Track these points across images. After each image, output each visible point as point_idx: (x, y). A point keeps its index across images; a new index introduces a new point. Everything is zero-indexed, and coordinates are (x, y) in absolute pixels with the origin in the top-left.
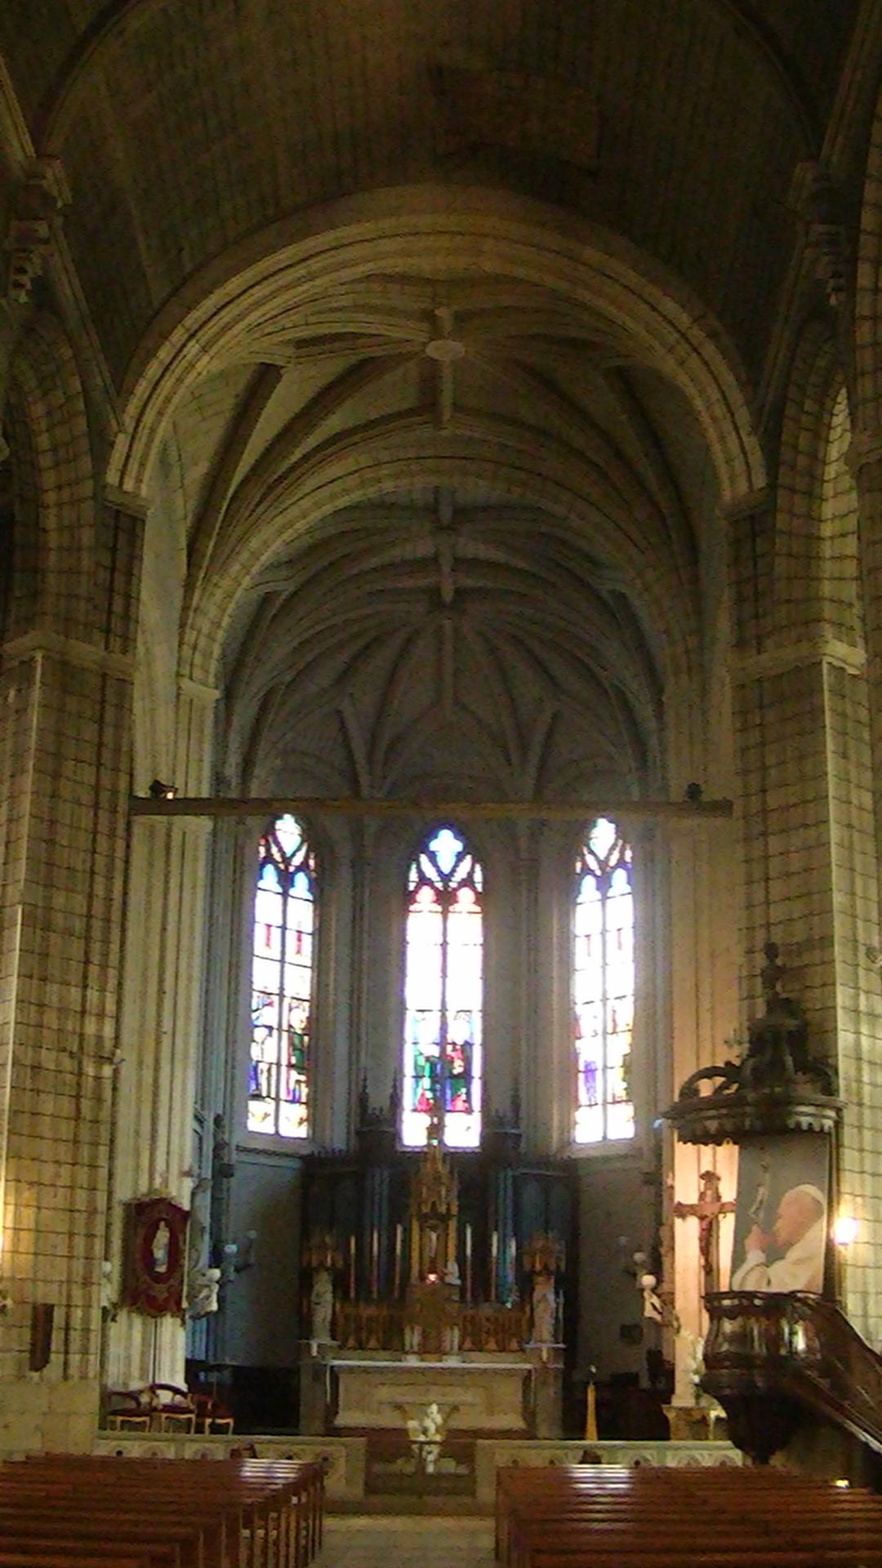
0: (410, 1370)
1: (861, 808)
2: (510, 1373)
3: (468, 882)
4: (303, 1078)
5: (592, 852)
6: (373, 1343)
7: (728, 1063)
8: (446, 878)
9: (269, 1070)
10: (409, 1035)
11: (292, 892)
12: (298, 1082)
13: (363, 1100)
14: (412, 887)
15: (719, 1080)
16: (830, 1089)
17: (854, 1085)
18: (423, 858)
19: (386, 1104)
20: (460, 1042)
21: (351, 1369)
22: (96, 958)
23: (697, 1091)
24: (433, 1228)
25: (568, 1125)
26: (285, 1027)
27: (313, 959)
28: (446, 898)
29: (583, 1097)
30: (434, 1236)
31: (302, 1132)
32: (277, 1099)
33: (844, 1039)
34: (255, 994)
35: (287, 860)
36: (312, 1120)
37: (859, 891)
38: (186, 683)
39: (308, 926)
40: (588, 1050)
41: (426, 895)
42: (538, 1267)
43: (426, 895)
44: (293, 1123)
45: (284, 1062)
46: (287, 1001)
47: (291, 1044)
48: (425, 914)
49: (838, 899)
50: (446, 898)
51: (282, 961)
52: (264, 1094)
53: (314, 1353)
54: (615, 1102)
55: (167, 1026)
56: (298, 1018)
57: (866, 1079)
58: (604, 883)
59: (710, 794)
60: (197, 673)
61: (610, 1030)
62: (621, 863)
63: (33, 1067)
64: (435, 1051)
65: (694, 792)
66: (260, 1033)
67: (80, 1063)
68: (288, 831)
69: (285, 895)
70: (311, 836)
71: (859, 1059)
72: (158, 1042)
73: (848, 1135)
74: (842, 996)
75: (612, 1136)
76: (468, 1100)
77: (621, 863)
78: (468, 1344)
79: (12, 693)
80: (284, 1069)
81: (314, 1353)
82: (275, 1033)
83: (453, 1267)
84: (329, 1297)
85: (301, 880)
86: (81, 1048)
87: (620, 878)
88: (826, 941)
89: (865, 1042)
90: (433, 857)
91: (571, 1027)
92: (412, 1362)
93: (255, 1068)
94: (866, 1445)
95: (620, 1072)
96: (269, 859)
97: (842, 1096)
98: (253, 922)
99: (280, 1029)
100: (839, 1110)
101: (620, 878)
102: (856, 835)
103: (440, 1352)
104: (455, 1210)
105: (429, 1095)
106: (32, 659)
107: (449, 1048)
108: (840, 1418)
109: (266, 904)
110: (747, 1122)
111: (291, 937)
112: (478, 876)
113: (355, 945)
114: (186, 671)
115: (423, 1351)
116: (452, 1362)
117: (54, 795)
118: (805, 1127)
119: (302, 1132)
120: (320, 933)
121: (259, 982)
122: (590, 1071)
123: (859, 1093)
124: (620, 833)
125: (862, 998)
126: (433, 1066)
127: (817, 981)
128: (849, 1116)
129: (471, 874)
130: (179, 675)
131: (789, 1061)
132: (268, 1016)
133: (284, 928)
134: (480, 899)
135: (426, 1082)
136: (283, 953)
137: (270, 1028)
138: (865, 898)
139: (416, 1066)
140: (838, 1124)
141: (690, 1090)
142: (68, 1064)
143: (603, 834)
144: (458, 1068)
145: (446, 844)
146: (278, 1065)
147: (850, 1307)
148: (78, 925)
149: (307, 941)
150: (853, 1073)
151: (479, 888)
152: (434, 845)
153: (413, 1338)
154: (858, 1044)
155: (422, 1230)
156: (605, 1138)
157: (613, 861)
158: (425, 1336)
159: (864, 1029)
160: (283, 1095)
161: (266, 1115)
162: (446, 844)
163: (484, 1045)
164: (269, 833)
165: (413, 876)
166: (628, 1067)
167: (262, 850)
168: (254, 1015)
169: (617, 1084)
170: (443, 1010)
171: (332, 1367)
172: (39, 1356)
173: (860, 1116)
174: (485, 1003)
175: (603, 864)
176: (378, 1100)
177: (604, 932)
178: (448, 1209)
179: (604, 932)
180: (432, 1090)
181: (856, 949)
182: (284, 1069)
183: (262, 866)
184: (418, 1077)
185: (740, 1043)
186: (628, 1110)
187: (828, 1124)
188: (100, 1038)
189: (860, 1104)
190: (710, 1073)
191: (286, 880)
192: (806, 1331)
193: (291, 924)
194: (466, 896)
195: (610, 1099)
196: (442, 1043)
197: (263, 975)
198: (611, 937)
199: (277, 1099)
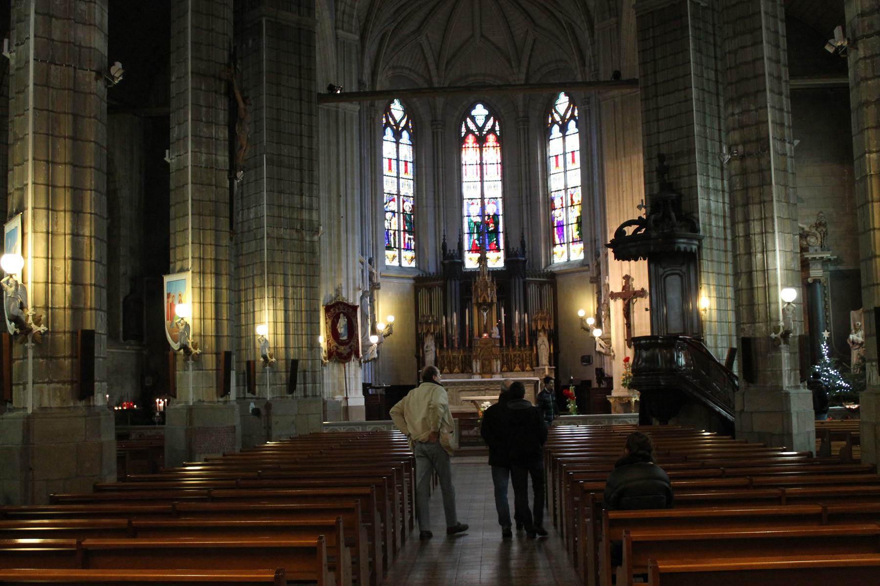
1: (708, 80)
3: (492, 131)
4: (412, 237)
5: (556, 112)
6: (456, 370)
7: (640, 218)
8: (481, 129)
9: (394, 234)
10: (465, 213)
11: (401, 141)
12: (409, 239)
13: (444, 247)
14: (463, 134)
15: (635, 227)
16: (694, 229)
17: (707, 227)
18: (468, 120)
19: (456, 248)
20: (492, 214)
22: (306, 180)
23: (625, 232)
24: (485, 310)
25: (550, 255)
28: (481, 141)
29: (557, 241)
31: (413, 264)
32: (399, 249)
33: (702, 203)
35: (397, 124)
36: (417, 258)
37: (708, 125)
38: (340, 32)
39: (410, 158)
40: (558, 215)
41: (471, 139)
43: (471, 139)
47: (404, 219)
49: (696, 128)
50: (481, 141)
51: (398, 177)
54: (573, 242)
55: (343, 213)
56: (408, 206)
57: (713, 224)
58: (564, 129)
59: (625, 76)
60: (346, 26)
61: (570, 204)
62: (572, 117)
63: (278, 239)
64: (479, 219)
65: (617, 75)
66: (389, 215)
67: (302, 235)
68: (397, 110)
69: (397, 143)
70: (407, 111)
71: (710, 213)
72: (339, 222)
73: (705, 253)
74: (700, 181)
75: (572, 259)
76: (498, 243)
77: (572, 117)
78: (505, 369)
79: (250, 42)
83: (496, 330)
84: (433, 348)
85: (405, 134)
86: (302, 227)
87: (572, 125)
88: (691, 152)
89: (713, 205)
90: (473, 119)
91: (550, 204)
92: (477, 378)
93: (387, 233)
94: (719, 413)
95: (575, 227)
96: (388, 124)
97: (701, 233)
98: (382, 157)
99: (398, 212)
100: (700, 240)
101: (572, 125)
102: (706, 95)
103: (491, 373)
104: (495, 300)
105: (477, 242)
106: (260, 24)
107: (486, 218)
108: (705, 400)
109: (388, 148)
110: (652, 248)
111: (402, 164)
112: (497, 128)
113: (435, 168)
114: (340, 24)
115: (483, 373)
117: (278, 95)
118: (682, 249)
119: (413, 264)
120: (416, 162)
121: (387, 189)
122: (560, 226)
123: (711, 232)
124: (571, 101)
125: (711, 181)
126: (478, 227)
127: (685, 173)
128: (705, 243)
129: (494, 126)
130: (336, 28)
131: (673, 214)
132: (393, 206)
133: (398, 160)
134: (499, 140)
135: (476, 236)
136: (398, 173)
137: (393, 212)
138: (712, 128)
140: (700, 247)
141: (620, 232)
142: (295, 235)
143: (562, 102)
144: (491, 227)
145: (480, 112)
146: (399, 231)
147: (708, 342)
148: (296, 163)
149: (410, 166)
150: (707, 220)
151: (498, 133)
152: (473, 113)
153: (477, 366)
154: (709, 205)
155: (479, 311)
156: (569, 260)
157: (568, 116)
158: (483, 366)
159: (712, 198)
160: (402, 247)
161: (394, 257)
162: (480, 112)
163: (504, 215)
164: (388, 110)
165: (464, 129)
166: (579, 222)
167: (384, 120)
169: (573, 232)
170: (482, 198)
172: (291, 386)
173: (711, 242)
174: (504, 192)
175: (563, 118)
176: (452, 246)
177: (565, 154)
179: (565, 154)
180: (478, 239)
181: (707, 156)
183: (385, 128)
184: (470, 234)
185: (645, 207)
186: (581, 246)
187: (694, 247)
188: (311, 221)
189: (711, 237)
190: (629, 223)
191: (397, 135)
192: (685, 356)
193: (402, 158)
194: (491, 138)
196: (482, 214)
197: (389, 186)
198: (569, 157)
199: (399, 249)
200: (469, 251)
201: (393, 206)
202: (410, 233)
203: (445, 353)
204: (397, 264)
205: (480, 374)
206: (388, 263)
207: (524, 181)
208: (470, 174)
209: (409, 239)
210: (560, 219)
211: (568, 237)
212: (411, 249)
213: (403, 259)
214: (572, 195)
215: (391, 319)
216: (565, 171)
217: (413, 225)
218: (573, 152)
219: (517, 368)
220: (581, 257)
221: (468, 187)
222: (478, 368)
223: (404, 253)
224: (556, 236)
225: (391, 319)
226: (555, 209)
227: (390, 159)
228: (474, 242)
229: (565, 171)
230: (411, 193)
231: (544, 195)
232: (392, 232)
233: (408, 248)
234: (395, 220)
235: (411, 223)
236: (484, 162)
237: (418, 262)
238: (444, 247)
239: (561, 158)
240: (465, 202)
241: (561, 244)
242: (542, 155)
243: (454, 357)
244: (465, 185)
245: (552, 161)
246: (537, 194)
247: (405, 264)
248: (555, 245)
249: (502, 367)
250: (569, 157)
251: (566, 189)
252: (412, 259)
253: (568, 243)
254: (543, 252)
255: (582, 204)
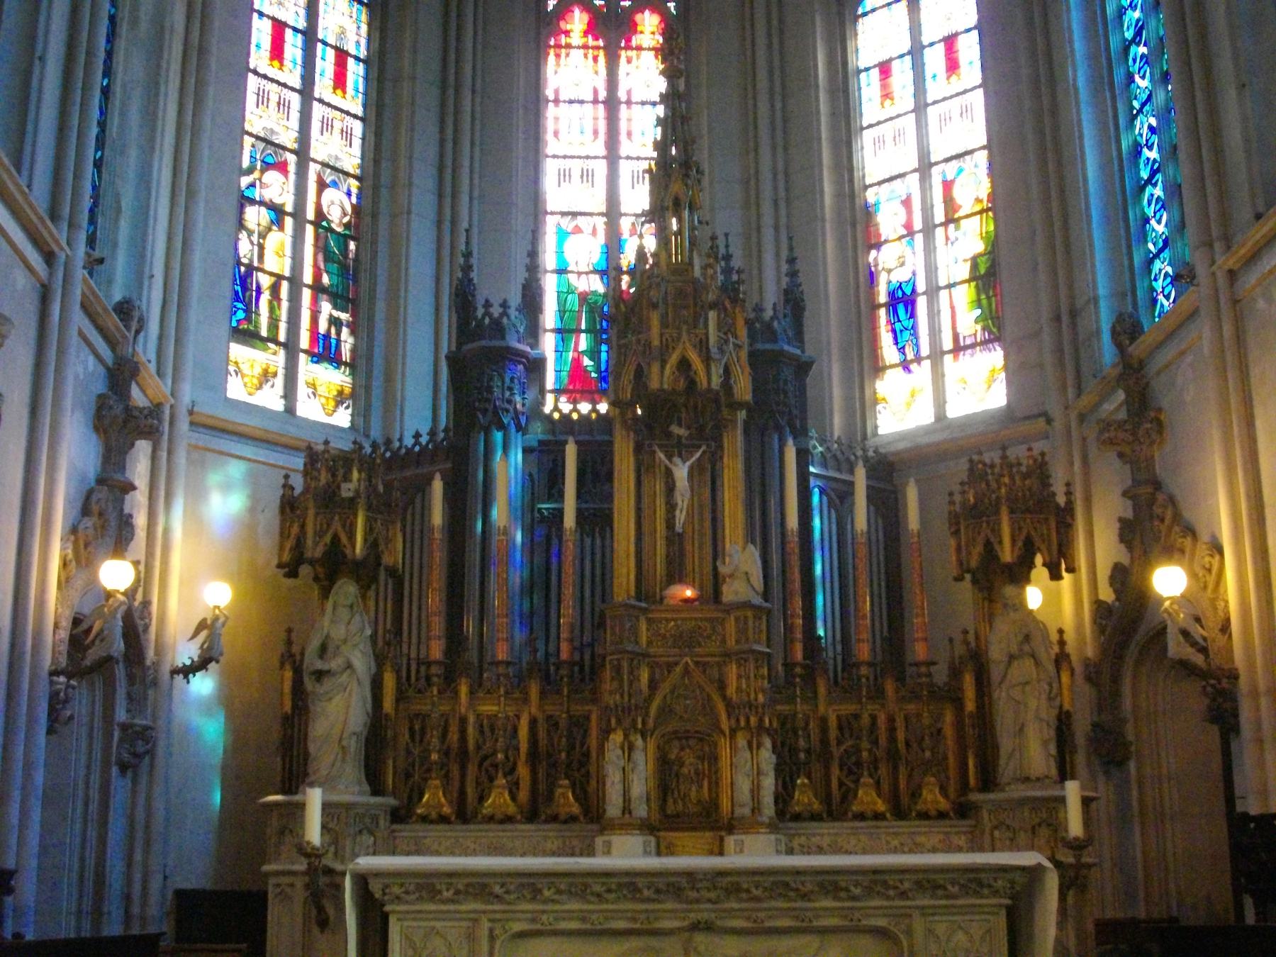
0: (629, 883)
2: (973, 880)
4: (344, 316)
6: (499, 799)
9: (275, 289)
10: (549, 260)
12: (334, 321)
13: (464, 297)
19: (515, 299)
21: (428, 886)
24: (679, 449)
26: (311, 215)
27: (365, 106)
29: (889, 353)
30: (681, 472)
31: (343, 418)
32: (291, 347)
34: (248, 141)
36: (357, 397)
40: (895, 262)
42: (1007, 554)
44: (323, 399)
45: (308, 278)
46: (313, 169)
47: (321, 246)
48: (577, 54)
51: (306, 91)
52: (264, 333)
53: (314, 833)
54: (958, 349)
56: (338, 205)
61: (939, 216)
64: (596, 285)
66: (255, 216)
75: (954, 411)
78: (804, 797)
80: (307, 294)
81: (314, 833)
82: (289, 222)
84: (361, 662)
91: (859, 227)
92: (626, 853)
93: (244, 281)
95: (965, 295)
99: (298, 214)
103: (715, 823)
104: (743, 387)
105: (587, 362)
111: (325, 64)
115: (673, 815)
116: (755, 852)
119: (343, 418)
120: (380, 65)
121: (258, 119)
122: (903, 300)
132: (278, 188)
133: (310, 36)
135: (584, 342)
137: (278, 212)
139: (562, 312)
146: (295, 281)
149: (355, 71)
153: (627, 774)
156: (940, 416)
160: (304, 342)
161: (266, 376)
166: (987, 277)
168: (244, 181)
169: (962, 311)
171: (362, 880)
177: (916, 52)
178: (727, 385)
179: (916, 52)
180: (594, 354)
182: (307, 294)
186: (995, 357)
193: (328, 28)
195: (948, 344)
196: (610, 271)
197: (266, 116)
198: (935, 59)
199: (291, 347)
200: (558, 392)
201: (278, 188)
202: (339, 300)
203: (432, 704)
204: (278, 405)
205: (647, 827)
206: (236, 389)
207: (765, 151)
208: (569, 131)
209: (334, 321)
210: (900, 276)
211: (935, 332)
212: (336, 360)
213: (302, 391)
214: (948, 186)
215: (219, 595)
216: (920, 107)
217: (355, 267)
218: (950, 42)
219: (868, 797)
220: (995, 397)
221: (564, 176)
222: (638, 788)
223: (307, 369)
224: (886, 338)
225: (219, 595)
226: (878, 246)
227: (279, 27)
228: (577, 362)
229: (920, 107)
230: (351, 159)
231: (839, 195)
232: (265, 281)
233: (325, 352)
234: (279, 243)
235: (344, 268)
236: (622, 94)
237: (362, 414)
238: (464, 297)
239: (902, 74)
240: (551, 223)
241: (905, 366)
242: (831, 63)
243: (488, 726)
244: (550, 169)
245: (869, 87)
246: (814, 189)
247: (310, 409)
248: (878, 369)
249: (783, 797)
250: (935, 59)
251: (925, 167)
252: (340, 399)
253: (937, 355)
254: (837, 392)
255: (997, 205)
